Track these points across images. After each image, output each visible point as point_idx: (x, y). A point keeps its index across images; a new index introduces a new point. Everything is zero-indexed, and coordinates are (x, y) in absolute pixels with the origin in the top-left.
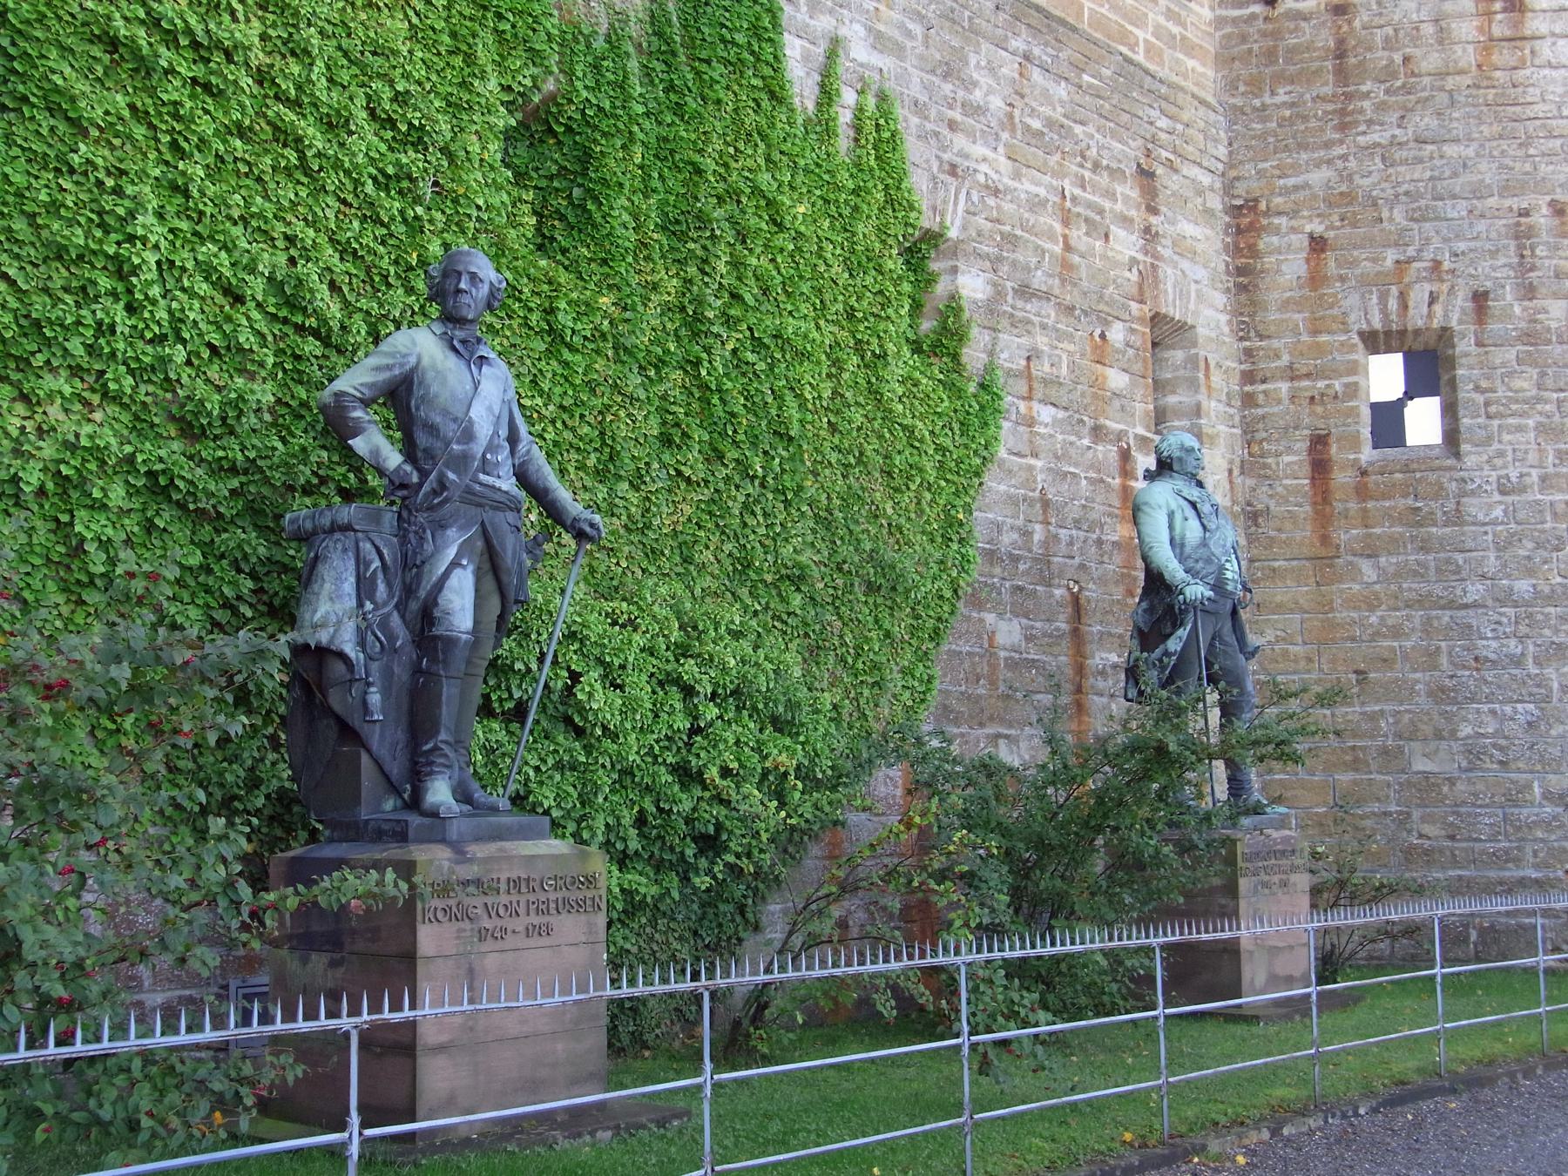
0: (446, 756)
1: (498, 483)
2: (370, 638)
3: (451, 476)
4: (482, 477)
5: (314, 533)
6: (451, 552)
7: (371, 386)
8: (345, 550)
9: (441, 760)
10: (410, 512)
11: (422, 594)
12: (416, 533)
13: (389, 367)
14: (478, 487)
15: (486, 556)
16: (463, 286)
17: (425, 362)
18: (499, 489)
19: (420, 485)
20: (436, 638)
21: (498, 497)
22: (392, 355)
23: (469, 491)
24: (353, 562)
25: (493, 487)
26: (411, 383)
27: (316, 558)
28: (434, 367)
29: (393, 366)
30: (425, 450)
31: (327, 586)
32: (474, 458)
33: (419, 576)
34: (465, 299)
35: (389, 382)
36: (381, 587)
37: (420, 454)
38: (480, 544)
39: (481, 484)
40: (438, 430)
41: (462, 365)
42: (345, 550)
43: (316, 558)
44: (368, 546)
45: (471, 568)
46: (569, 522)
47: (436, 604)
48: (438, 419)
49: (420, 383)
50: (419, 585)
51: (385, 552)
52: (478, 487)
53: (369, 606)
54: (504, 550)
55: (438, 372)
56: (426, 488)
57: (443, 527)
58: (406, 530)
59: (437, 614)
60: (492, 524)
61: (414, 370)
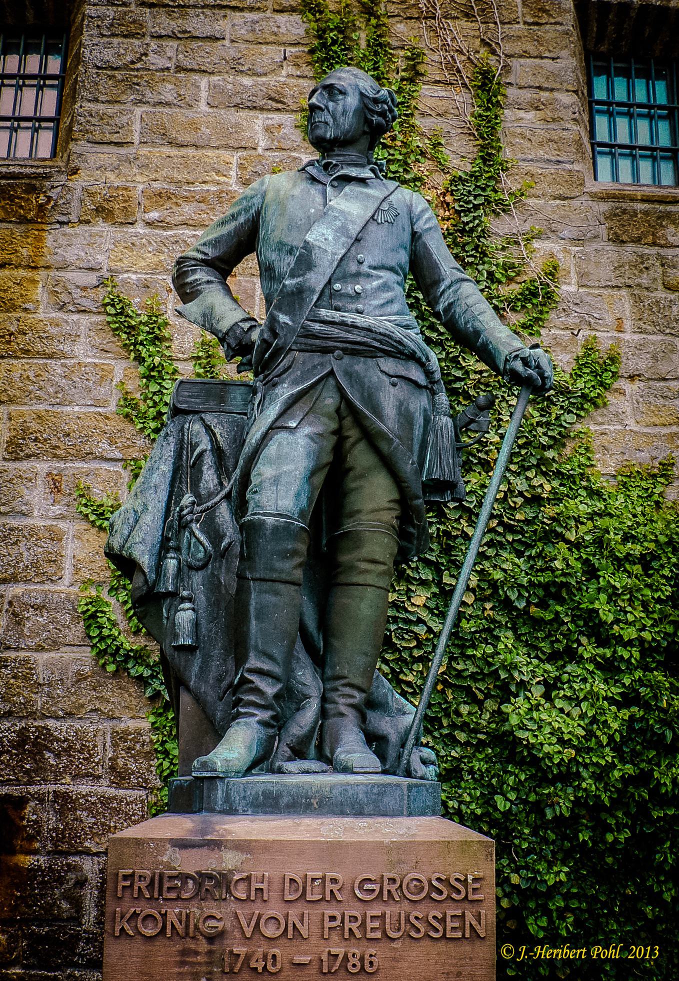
0: (257, 691)
3: (283, 318)
4: (323, 312)
6: (272, 412)
9: (252, 698)
13: (234, 217)
14: (317, 326)
18: (354, 326)
23: (309, 335)
25: (343, 324)
29: (239, 213)
32: (313, 291)
36: (209, 477)
44: (197, 427)
52: (317, 326)
53: (188, 499)
57: (275, 385)
61: (258, 213)
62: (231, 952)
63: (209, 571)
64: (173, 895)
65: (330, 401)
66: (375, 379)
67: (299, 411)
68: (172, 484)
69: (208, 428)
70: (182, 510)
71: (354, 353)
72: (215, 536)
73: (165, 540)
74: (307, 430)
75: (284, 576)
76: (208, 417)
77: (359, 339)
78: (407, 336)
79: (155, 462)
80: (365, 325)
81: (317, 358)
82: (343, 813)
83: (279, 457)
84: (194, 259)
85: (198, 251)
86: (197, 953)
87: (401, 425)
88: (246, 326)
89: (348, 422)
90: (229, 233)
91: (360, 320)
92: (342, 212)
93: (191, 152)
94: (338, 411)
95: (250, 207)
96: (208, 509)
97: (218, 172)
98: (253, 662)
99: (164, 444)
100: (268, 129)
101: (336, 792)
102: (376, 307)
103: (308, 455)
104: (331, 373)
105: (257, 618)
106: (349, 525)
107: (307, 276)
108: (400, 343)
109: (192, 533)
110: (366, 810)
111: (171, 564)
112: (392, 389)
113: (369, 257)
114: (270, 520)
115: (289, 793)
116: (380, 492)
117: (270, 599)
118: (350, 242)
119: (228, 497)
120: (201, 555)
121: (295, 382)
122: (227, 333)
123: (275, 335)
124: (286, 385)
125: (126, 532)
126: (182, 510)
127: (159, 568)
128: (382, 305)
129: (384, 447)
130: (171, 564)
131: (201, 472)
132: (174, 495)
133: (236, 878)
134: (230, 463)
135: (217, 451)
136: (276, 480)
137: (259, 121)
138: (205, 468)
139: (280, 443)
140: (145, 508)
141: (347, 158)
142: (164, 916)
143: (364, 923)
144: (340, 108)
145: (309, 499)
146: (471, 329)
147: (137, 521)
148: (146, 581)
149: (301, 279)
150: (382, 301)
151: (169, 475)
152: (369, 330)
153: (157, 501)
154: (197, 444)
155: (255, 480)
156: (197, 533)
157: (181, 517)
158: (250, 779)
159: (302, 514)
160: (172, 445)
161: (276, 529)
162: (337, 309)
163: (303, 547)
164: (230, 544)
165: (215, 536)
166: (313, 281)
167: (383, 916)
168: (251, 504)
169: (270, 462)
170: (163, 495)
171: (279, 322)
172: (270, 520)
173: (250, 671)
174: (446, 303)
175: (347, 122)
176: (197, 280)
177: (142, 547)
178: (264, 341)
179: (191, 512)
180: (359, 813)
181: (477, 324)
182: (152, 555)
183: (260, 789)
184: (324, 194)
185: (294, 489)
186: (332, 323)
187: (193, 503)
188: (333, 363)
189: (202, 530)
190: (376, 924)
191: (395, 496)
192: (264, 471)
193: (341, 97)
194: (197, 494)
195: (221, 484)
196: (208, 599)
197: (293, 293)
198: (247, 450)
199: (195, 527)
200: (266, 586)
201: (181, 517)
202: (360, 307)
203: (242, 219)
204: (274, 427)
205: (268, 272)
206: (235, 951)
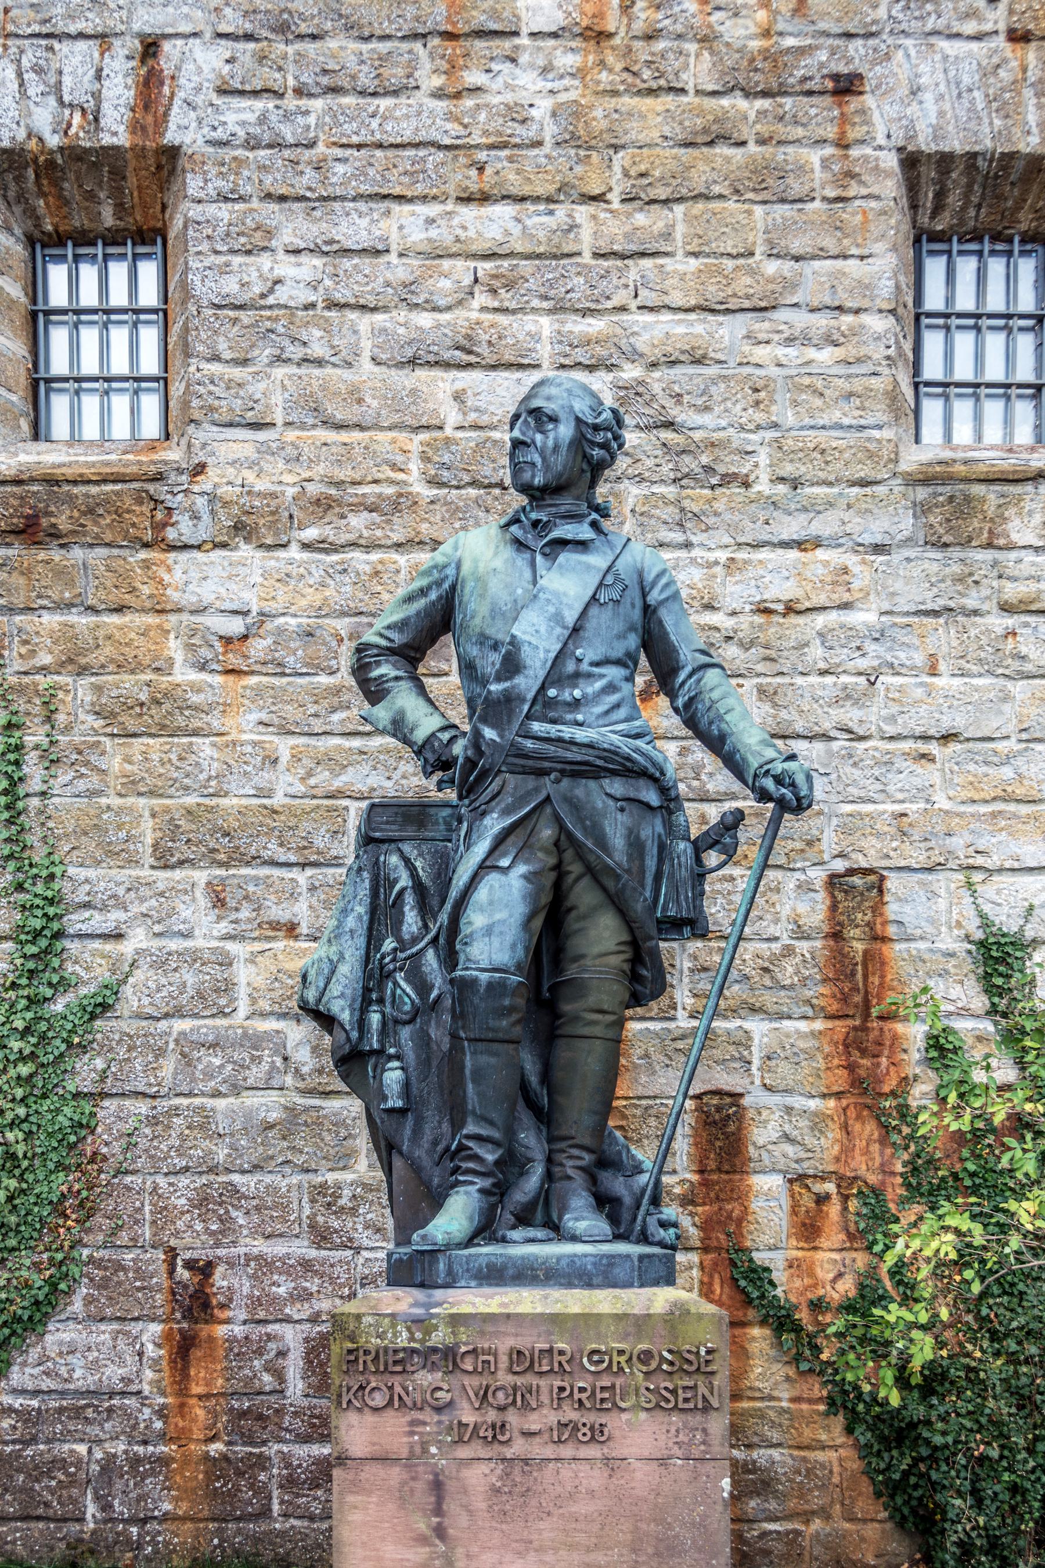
4: (536, 727)
6: (481, 848)
14: (529, 744)
18: (572, 742)
24: (367, 884)
25: (560, 740)
44: (394, 859)
51: (418, 864)
52: (529, 744)
53: (389, 944)
57: (484, 814)
62: (460, 1423)
64: (399, 1368)
65: (547, 833)
66: (600, 804)
67: (511, 846)
68: (370, 929)
69: (407, 862)
70: (383, 957)
71: (575, 775)
72: (423, 987)
73: (367, 990)
74: (522, 869)
75: (500, 1035)
76: (407, 848)
78: (637, 750)
80: (586, 740)
81: (531, 782)
82: (570, 1285)
83: (491, 903)
86: (425, 1424)
87: (630, 857)
88: (445, 736)
89: (569, 855)
91: (581, 735)
92: (556, 594)
93: (356, 435)
94: (556, 844)
96: (413, 955)
97: (394, 467)
98: (471, 1128)
101: (564, 1263)
102: (599, 717)
103: (524, 897)
104: (548, 799)
105: (474, 1081)
106: (572, 971)
108: (629, 759)
109: (396, 984)
110: (595, 1281)
111: (375, 1018)
112: (619, 816)
113: (587, 652)
114: (484, 977)
115: (514, 1265)
116: (607, 934)
117: (484, 1059)
119: (435, 940)
120: (407, 1008)
121: (506, 812)
122: (423, 746)
123: (480, 753)
124: (495, 815)
125: (322, 985)
126: (383, 957)
127: (362, 1024)
128: (607, 713)
130: (375, 1018)
131: (403, 914)
132: (373, 941)
133: (463, 1349)
134: (435, 902)
135: (419, 887)
136: (489, 931)
137: (446, 382)
138: (407, 908)
140: (342, 957)
141: (563, 509)
142: (391, 1388)
143: (593, 1393)
145: (527, 949)
147: (333, 972)
148: (348, 1039)
150: (606, 707)
151: (366, 918)
152: (590, 746)
153: (353, 950)
154: (396, 881)
155: (465, 930)
156: (402, 983)
157: (382, 968)
158: (472, 1250)
159: (519, 967)
161: (490, 985)
162: (554, 722)
163: (521, 1002)
164: (439, 996)
165: (423, 987)
167: (613, 1386)
168: (462, 957)
170: (361, 941)
172: (484, 977)
173: (468, 1137)
175: (559, 462)
177: (341, 1002)
178: (467, 759)
179: (394, 960)
180: (589, 1285)
182: (353, 1011)
183: (483, 1261)
184: (533, 564)
185: (509, 939)
187: (395, 950)
188: (548, 785)
189: (407, 980)
190: (606, 1395)
191: (625, 937)
192: (475, 919)
194: (399, 939)
195: (426, 926)
196: (418, 1056)
198: (454, 893)
199: (400, 977)
200: (480, 1046)
201: (382, 967)
202: (580, 717)
204: (485, 867)
205: (468, 669)
206: (464, 1420)
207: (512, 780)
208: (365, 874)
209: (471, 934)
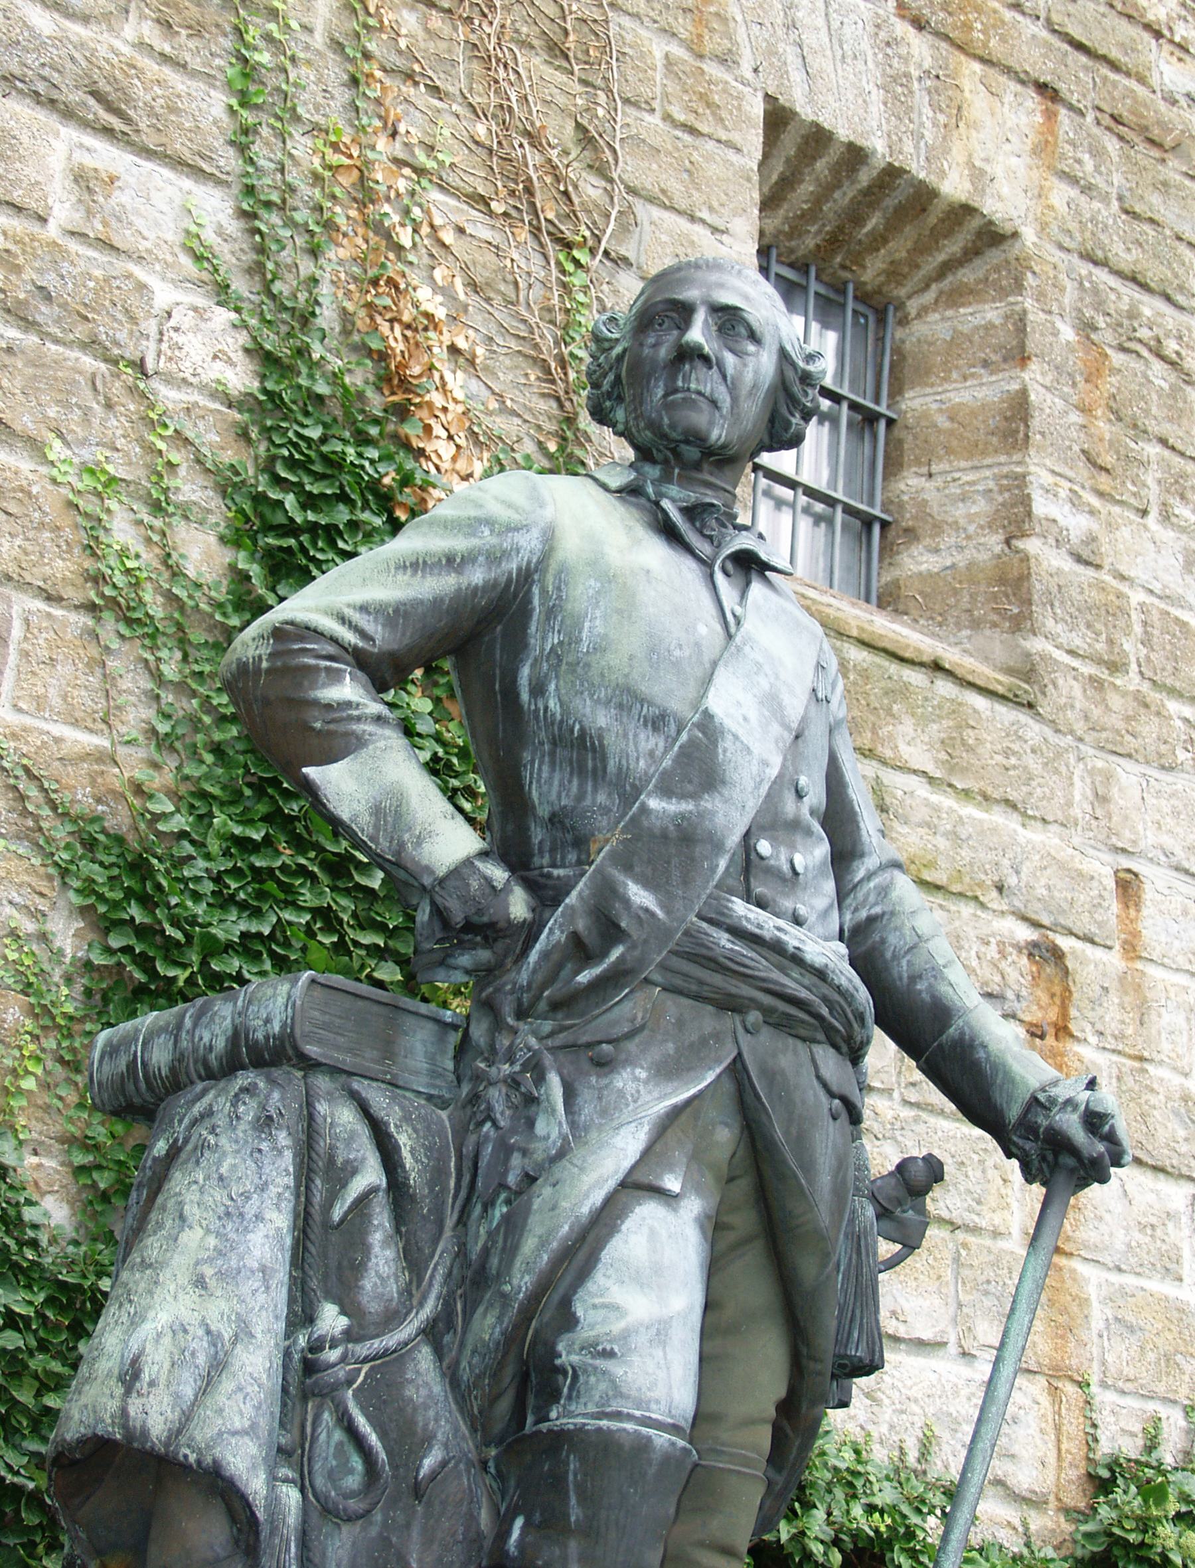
1: (793, 937)
2: (329, 1436)
3: (639, 895)
4: (740, 907)
5: (175, 1082)
7: (395, 615)
8: (265, 1123)
10: (498, 1024)
11: (521, 1282)
12: (514, 1083)
13: (451, 562)
14: (723, 939)
15: (744, 1185)
16: (697, 334)
17: (570, 547)
18: (797, 959)
19: (531, 931)
20: (560, 1438)
21: (792, 984)
22: (471, 526)
24: (288, 1159)
25: (776, 948)
26: (525, 612)
27: (174, 1152)
28: (595, 563)
29: (468, 559)
30: (556, 820)
31: (191, 1238)
32: (718, 846)
33: (514, 1226)
34: (703, 381)
35: (462, 601)
37: (538, 835)
38: (725, 1136)
39: (738, 932)
40: (600, 753)
41: (688, 569)
42: (265, 1123)
43: (174, 1152)
44: (346, 1117)
45: (693, 1207)
46: (1013, 1113)
47: (567, 1320)
48: (602, 719)
49: (550, 613)
50: (511, 1251)
51: (404, 1140)
53: (331, 1319)
54: (809, 1167)
55: (608, 578)
56: (552, 935)
57: (604, 1065)
58: (478, 1077)
59: (568, 1355)
60: (770, 1075)
61: (526, 576)
63: (374, 1531)
77: (803, 994)
79: (247, 1196)
81: (708, 1020)
84: (334, 640)
85: (343, 620)
90: (437, 602)
95: (506, 554)
96: (386, 1353)
99: (264, 1146)
100: (82, 179)
107: (707, 803)
118: (789, 737)
121: (668, 1071)
125: (188, 1392)
126: (316, 1346)
129: (807, 1268)
131: (366, 1249)
138: (376, 1238)
139: (652, 1232)
140: (243, 1332)
144: (749, 377)
146: (926, 997)
147: (218, 1366)
149: (687, 806)
154: (352, 1170)
160: (288, 1155)
162: (761, 904)
166: (720, 820)
169: (639, 1279)
171: (627, 902)
174: (863, 914)
176: (349, 704)
179: (343, 1359)
181: (943, 989)
186: (753, 939)
193: (751, 348)
197: (664, 836)
203: (477, 576)
207: (674, 1007)
208: (283, 1138)
209: (625, 1335)
